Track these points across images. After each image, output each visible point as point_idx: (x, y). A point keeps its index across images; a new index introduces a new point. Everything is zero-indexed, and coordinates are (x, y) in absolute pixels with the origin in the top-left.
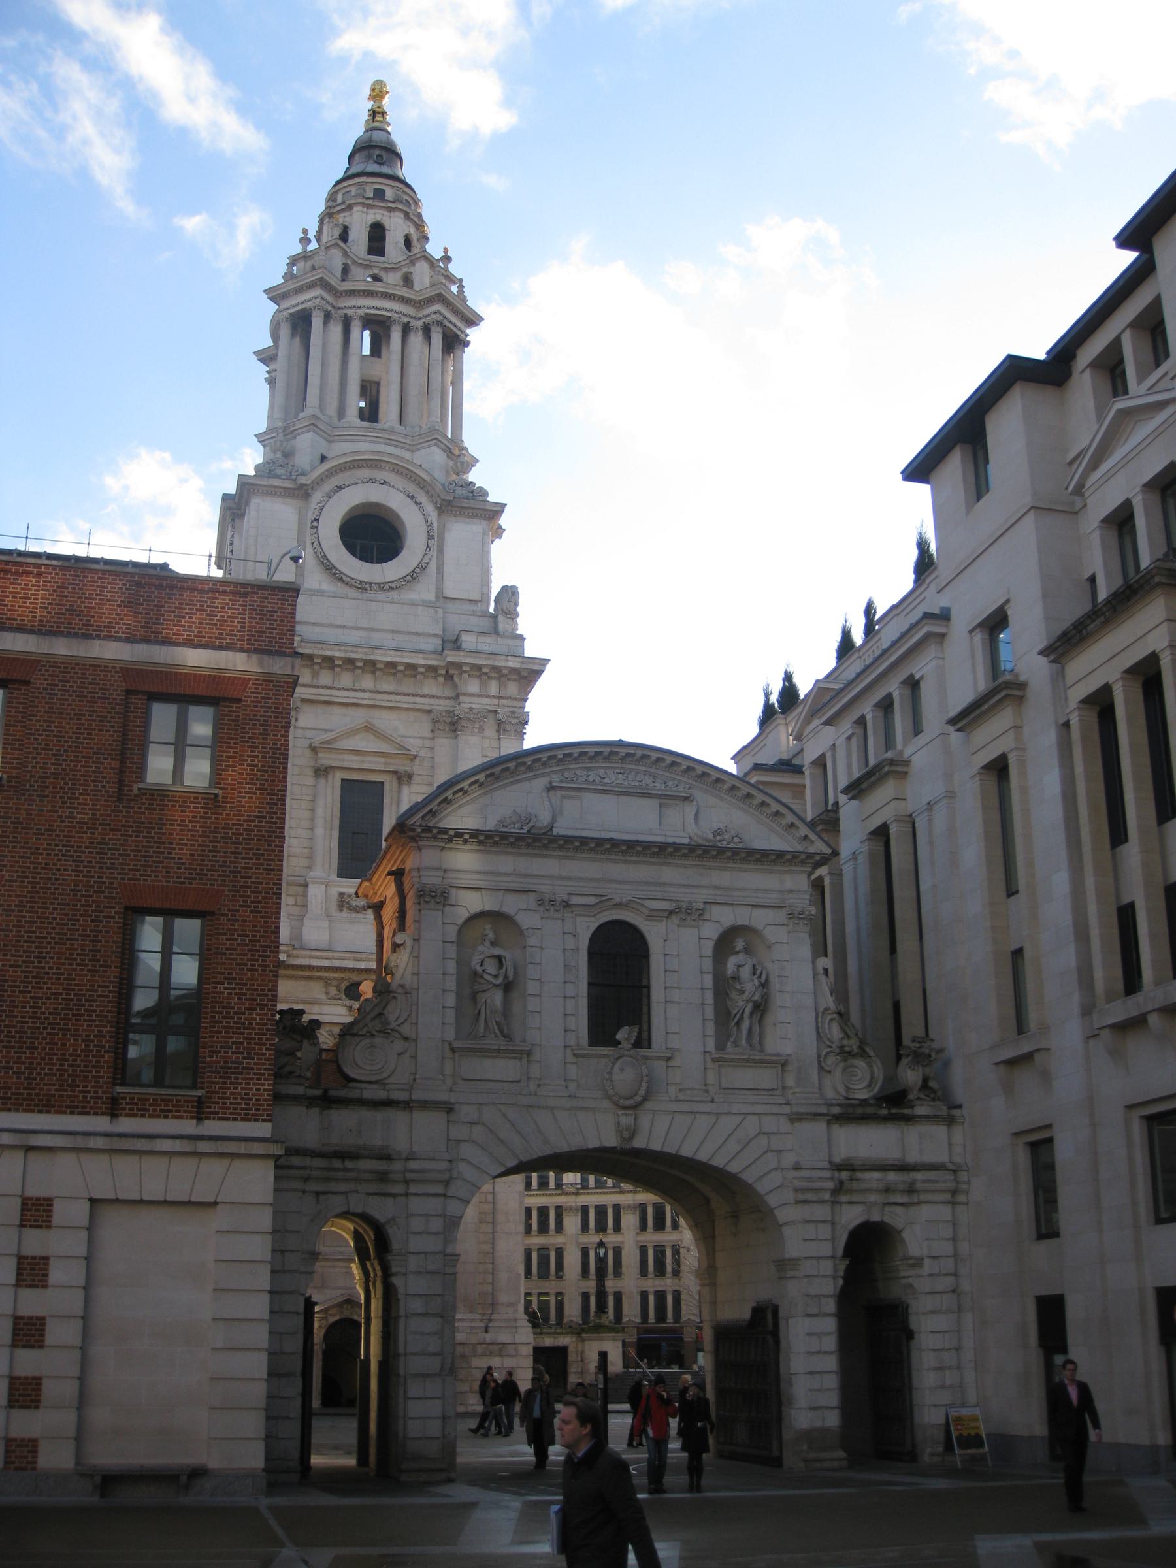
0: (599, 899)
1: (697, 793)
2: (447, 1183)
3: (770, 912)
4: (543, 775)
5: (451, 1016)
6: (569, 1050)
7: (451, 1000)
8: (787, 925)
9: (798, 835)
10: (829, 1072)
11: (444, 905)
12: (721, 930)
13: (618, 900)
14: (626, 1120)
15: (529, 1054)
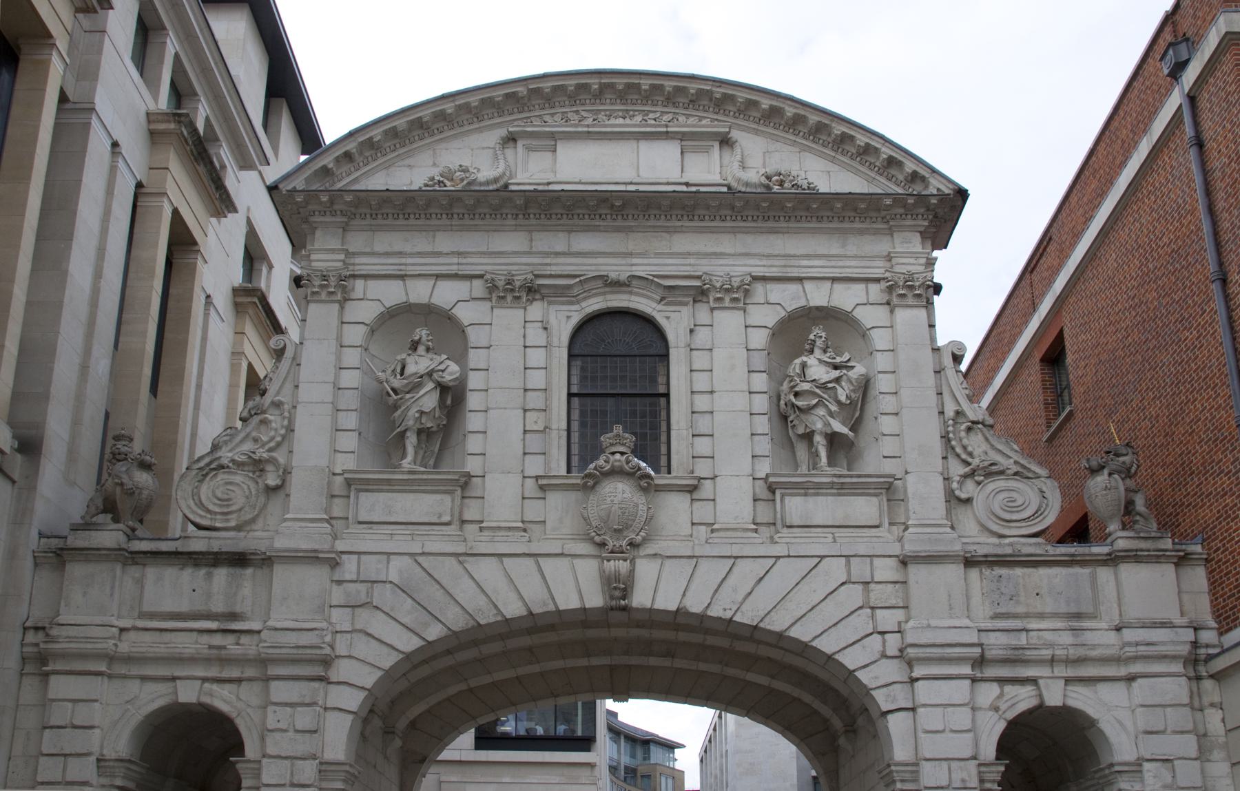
0: (578, 280)
1: (735, 134)
2: (327, 662)
3: (861, 286)
4: (499, 125)
5: (349, 441)
6: (530, 483)
7: (350, 421)
8: (888, 303)
9: (901, 177)
10: (968, 501)
11: (346, 300)
12: (783, 314)
13: (613, 275)
14: (623, 566)
15: (465, 486)
